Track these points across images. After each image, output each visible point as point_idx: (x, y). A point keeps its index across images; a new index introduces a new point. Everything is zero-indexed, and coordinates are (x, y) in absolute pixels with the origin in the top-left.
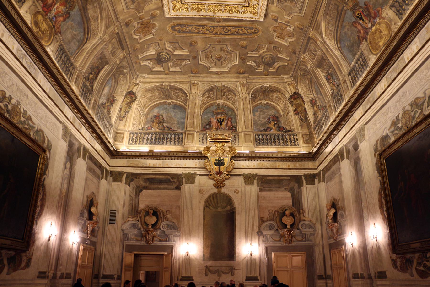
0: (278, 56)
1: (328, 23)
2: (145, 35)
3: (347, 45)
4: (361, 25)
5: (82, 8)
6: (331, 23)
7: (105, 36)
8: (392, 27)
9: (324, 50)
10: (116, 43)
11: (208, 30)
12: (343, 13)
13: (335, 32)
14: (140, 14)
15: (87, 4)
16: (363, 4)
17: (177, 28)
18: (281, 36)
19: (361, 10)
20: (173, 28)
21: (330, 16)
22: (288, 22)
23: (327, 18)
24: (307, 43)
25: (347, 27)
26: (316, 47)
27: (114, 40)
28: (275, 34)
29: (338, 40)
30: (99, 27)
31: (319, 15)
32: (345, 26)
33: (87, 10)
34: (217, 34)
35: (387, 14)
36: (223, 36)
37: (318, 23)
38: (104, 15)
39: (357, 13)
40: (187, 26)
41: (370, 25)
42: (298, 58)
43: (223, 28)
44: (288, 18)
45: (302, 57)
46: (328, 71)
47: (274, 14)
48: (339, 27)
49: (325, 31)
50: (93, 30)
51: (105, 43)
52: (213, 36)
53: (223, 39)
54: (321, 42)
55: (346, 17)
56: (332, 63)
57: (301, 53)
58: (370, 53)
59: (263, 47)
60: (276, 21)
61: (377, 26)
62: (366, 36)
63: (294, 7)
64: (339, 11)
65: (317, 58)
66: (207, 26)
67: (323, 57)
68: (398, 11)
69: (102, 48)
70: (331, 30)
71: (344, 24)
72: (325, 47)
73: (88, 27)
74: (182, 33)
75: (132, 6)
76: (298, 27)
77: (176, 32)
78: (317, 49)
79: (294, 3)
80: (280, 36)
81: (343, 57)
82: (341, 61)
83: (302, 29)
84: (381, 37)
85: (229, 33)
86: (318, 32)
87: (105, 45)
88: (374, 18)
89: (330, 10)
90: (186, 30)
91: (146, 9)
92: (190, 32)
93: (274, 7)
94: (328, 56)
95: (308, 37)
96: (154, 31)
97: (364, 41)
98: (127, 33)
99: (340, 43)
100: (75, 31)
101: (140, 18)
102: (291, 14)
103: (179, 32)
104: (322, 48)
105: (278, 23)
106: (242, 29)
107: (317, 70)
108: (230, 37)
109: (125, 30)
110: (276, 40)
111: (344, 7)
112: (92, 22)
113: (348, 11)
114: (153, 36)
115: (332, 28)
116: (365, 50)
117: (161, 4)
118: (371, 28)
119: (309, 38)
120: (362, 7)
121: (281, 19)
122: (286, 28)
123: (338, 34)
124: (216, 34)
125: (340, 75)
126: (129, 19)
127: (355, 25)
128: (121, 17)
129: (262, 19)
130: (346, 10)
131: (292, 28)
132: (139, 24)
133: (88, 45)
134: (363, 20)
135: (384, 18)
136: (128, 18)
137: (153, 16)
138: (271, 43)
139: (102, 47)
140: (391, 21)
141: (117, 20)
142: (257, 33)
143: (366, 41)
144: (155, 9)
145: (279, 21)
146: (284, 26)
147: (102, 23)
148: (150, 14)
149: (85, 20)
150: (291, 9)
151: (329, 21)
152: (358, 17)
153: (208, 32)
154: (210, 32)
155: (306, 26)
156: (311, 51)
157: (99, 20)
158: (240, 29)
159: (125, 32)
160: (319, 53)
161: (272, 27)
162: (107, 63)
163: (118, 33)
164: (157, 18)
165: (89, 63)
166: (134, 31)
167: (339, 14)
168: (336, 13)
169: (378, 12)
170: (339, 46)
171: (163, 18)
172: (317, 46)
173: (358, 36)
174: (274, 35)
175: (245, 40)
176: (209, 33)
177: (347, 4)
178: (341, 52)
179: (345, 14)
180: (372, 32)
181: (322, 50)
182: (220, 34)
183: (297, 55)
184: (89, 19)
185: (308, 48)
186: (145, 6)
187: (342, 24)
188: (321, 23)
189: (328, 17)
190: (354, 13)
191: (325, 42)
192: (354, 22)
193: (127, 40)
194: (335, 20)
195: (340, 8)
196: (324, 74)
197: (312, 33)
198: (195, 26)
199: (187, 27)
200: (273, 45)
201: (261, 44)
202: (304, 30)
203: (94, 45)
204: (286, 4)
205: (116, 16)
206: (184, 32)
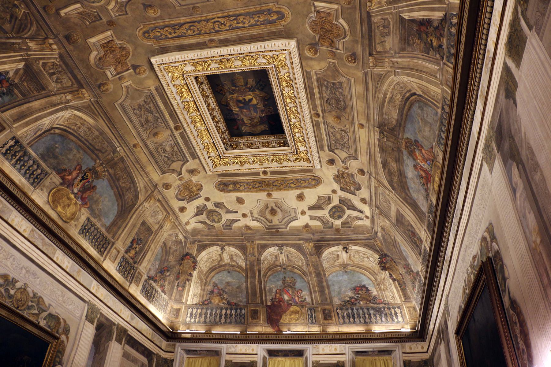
0: (78, 5)
1: (90, 129)
2: (329, 14)
3: (57, 147)
4: (76, 178)
5: (401, 129)
6: (88, 133)
7: (389, 69)
8: (73, 222)
9: (54, 98)
10: (377, 41)
11: (222, 24)
12: (94, 156)
13: (75, 134)
14: (333, 61)
15: (395, 126)
16: (95, 185)
17: (275, 17)
18: (107, 46)
19: (90, 180)
20: (282, 16)
21: (97, 137)
22: (120, 79)
23: (96, 132)
24: (75, 77)
25: (78, 156)
26: (64, 88)
27: (379, 49)
28: (118, 42)
29: (64, 133)
30: (392, 89)
31: (104, 124)
32: (79, 152)
33: (397, 121)
34: (205, 21)
35: (83, 215)
36: (195, 20)
37: (95, 115)
38: (381, 96)
39: (89, 175)
40: (259, 23)
41: (76, 191)
42: (56, 36)
43: (200, 31)
44: (126, 84)
45: (55, 47)
46: (16, 86)
47: (145, 75)
48: (79, 142)
49: (81, 118)
50: (400, 93)
51: (392, 60)
52: (210, 17)
53: (192, 14)
54: (68, 101)
55: (88, 157)
56: (31, 104)
57: (63, 51)
58: (49, 190)
59: (117, 11)
60: (135, 67)
61: (74, 200)
62: (65, 184)
63: (131, 103)
64: (97, 152)
65: (44, 75)
66: (227, 30)
67: (44, 89)
68: (85, 229)
69: (400, 57)
70: (79, 128)
71: (81, 152)
72: (59, 104)
73: (405, 104)
74: (264, 11)
75: (343, 80)
76: (105, 84)
77: (274, 10)
78: (59, 86)
79: (137, 107)
80: (110, 45)
81: (39, 133)
82: (33, 126)
83: (99, 87)
84: (64, 208)
85: (187, 26)
86: (84, 107)
87: (393, 57)
88: (82, 199)
89: (103, 141)
90: (259, 17)
91: (323, 65)
92: (250, 15)
93: (151, 84)
94: (43, 101)
95: (85, 86)
96: (312, 15)
97: (61, 181)
98: (356, 42)
99: (60, 135)
100: (419, 122)
101: (334, 55)
102: (127, 92)
103: (270, 12)
104: (59, 97)
105: (129, 65)
106: (170, 33)
107: (20, 61)
108: (182, 20)
109: (359, 49)
110: (109, 33)
111: (100, 160)
112: (397, 103)
113: (94, 163)
114: (316, 4)
115: (82, 131)
116: (51, 181)
117: (304, 64)
118: (73, 193)
119: (81, 86)
120: (93, 181)
121: (130, 75)
122: (115, 69)
123: (72, 138)
124: (208, 21)
125: (11, 116)
126: (349, 65)
127: (78, 168)
128: (360, 74)
129: (153, 60)
130: (95, 161)
131: (110, 76)
132: (336, 45)
133: (415, 85)
134: (81, 181)
135: (80, 210)
136: (351, 67)
137: (314, 47)
138: (111, 24)
139: (399, 60)
140: (78, 219)
141: (366, 75)
142: (144, 33)
143: (61, 184)
144: (312, 59)
145: (132, 70)
146: (119, 69)
147: (387, 90)
148: (318, 54)
149: (404, 116)
150: (133, 98)
151: (92, 132)
152: (85, 175)
153: (222, 20)
154: (219, 22)
155: (101, 98)
156: (60, 72)
157: (388, 96)
158: (174, 35)
159: (360, 47)
160: (53, 86)
161: (131, 53)
162: (402, 20)
163: (371, 54)
164: (308, 41)
165: (426, 64)
166: (345, 37)
167: (96, 152)
168: (97, 147)
169: (86, 204)
170: (57, 131)
171: (300, 36)
172: (64, 90)
173: (65, 170)
174: (119, 40)
175: (155, 19)
176: (219, 20)
177: (101, 165)
178: (47, 131)
179: (92, 158)
180: (69, 194)
181: (55, 95)
182: (201, 21)
183: (61, 37)
184: (399, 110)
185: (67, 72)
186: (325, 70)
187: (83, 149)
188: (95, 119)
189: (96, 133)
190: (90, 170)
191: (66, 108)
192: (81, 167)
193: (359, 28)
194: (90, 141)
195: (100, 155)
196: (11, 74)
197: (87, 97)
198: (246, 25)
199: (258, 21)
200: (104, 20)
201: (124, 17)
202: (96, 88)
203: (408, 75)
204: (143, 99)
205: (367, 83)
206: (261, 12)
